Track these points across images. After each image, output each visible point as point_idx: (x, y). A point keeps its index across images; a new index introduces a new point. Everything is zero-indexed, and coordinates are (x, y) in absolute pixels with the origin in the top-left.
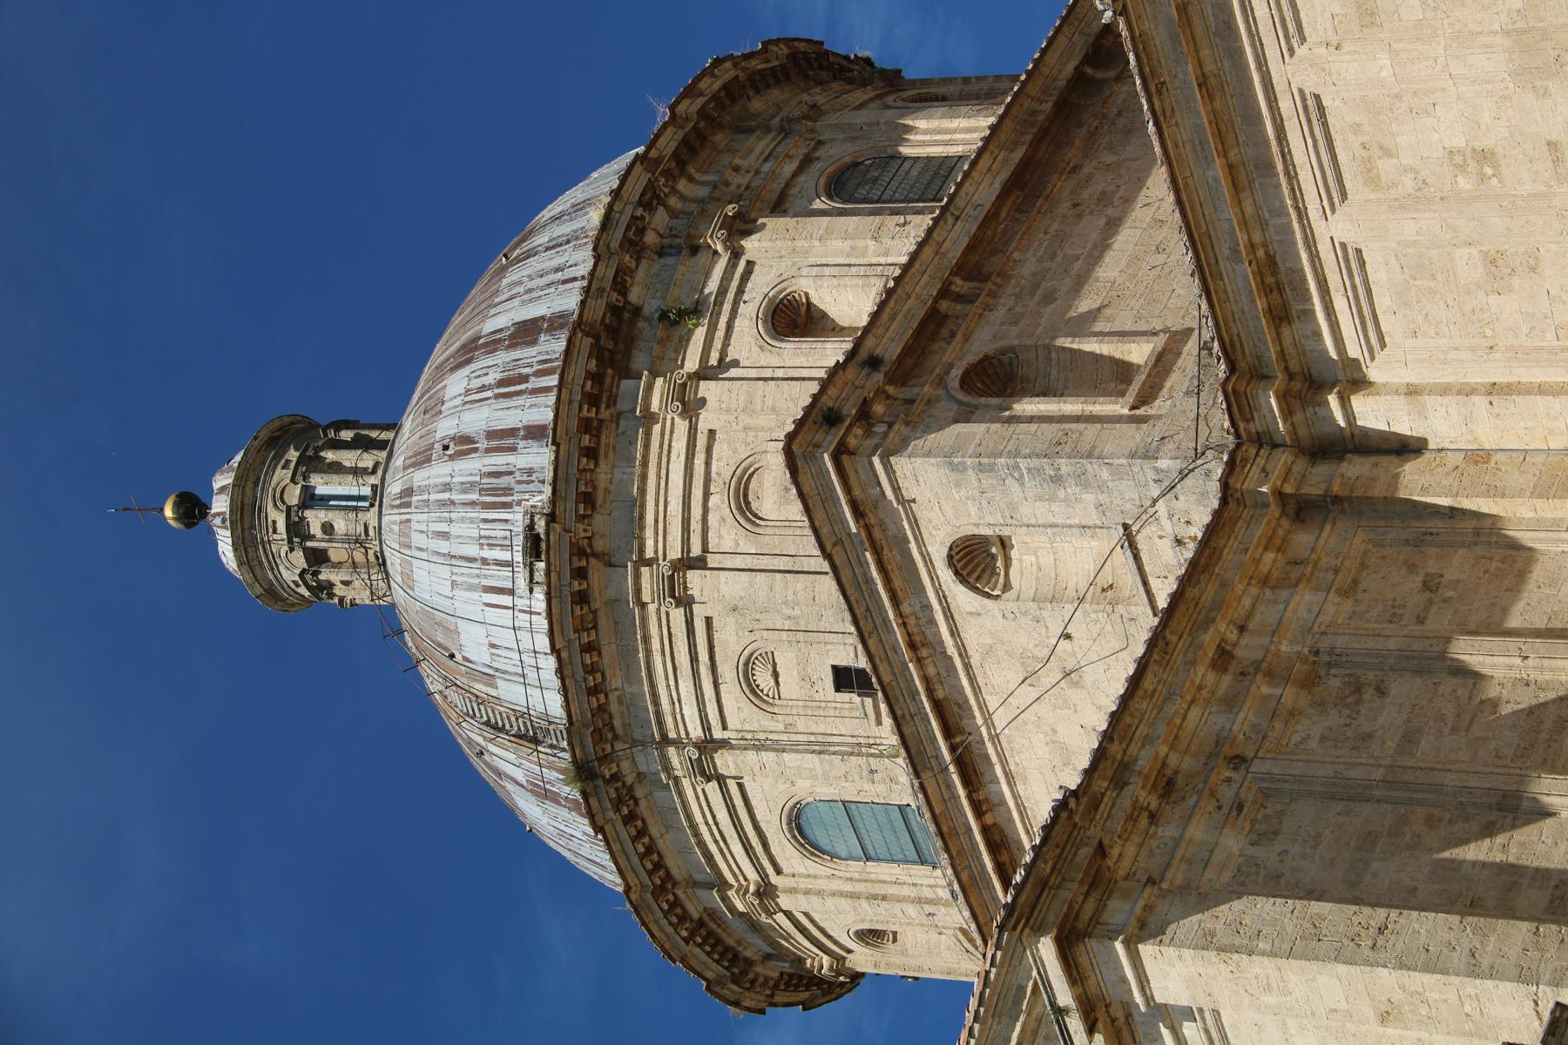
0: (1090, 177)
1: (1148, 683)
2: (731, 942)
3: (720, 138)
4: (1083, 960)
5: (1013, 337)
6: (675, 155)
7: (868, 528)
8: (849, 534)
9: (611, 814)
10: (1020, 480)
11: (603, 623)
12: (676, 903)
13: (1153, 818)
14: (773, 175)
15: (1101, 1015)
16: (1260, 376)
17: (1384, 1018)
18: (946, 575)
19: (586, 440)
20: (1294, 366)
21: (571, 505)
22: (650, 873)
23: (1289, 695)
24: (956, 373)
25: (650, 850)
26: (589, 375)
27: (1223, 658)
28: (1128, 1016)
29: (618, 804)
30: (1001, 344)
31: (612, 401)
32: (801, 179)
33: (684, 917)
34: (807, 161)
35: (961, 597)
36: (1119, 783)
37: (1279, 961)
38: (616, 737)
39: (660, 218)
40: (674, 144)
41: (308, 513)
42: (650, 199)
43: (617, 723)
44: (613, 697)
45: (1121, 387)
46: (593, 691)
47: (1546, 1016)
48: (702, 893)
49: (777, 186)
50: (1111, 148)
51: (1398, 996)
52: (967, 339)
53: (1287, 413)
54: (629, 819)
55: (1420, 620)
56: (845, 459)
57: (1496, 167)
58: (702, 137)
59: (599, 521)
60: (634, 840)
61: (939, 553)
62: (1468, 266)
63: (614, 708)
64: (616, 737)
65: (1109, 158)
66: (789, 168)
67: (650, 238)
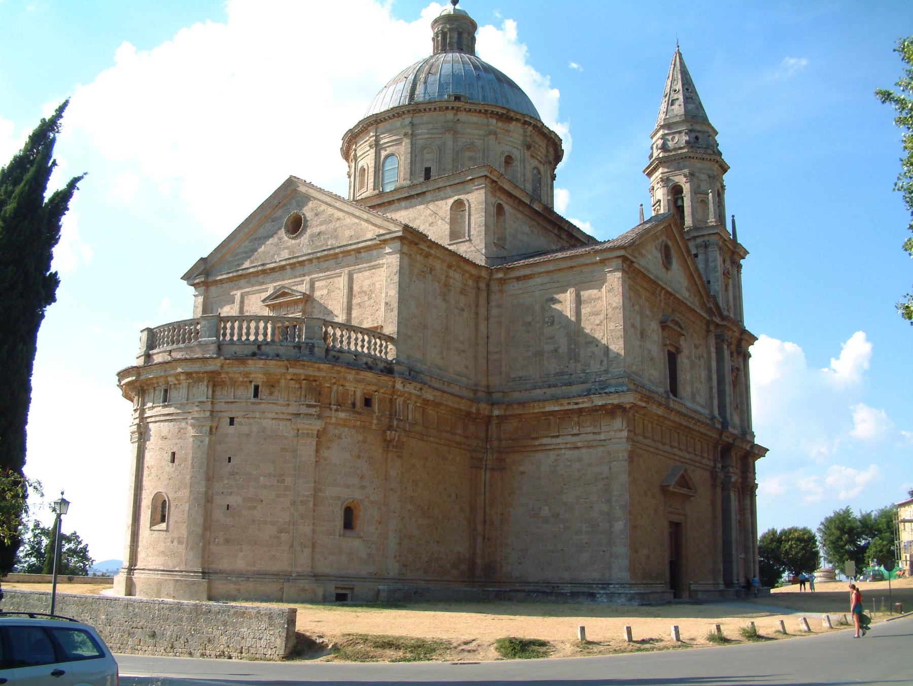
0: (536, 228)
1: (446, 252)
2: (361, 135)
3: (546, 141)
4: (395, 241)
5: (507, 214)
6: (543, 132)
7: (468, 181)
8: (467, 177)
9: (395, 112)
10: (479, 217)
11: (441, 113)
12: (372, 124)
13: (421, 254)
14: (537, 155)
15: (383, 242)
16: (505, 273)
17: (387, 304)
18: (456, 198)
19: (483, 111)
20: (507, 281)
21: (468, 107)
22: (380, 119)
23: (443, 282)
24: (501, 202)
25: (385, 119)
26: (498, 112)
27: (450, 267)
28: (381, 248)
29: (398, 114)
30: (506, 213)
31: (491, 117)
32: (537, 161)
33: (369, 126)
34: (540, 162)
35: (451, 201)
36: (428, 247)
37: (398, 284)
38: (413, 114)
39: (530, 128)
40: (545, 132)
41: (456, 33)
42: (535, 127)
43: (417, 115)
44: (423, 114)
45: (462, 209)
46: (425, 110)
47: (391, 335)
48: (374, 130)
49: (536, 156)
50: (542, 233)
51: (392, 307)
52: (507, 203)
53: (497, 279)
54: (394, 116)
55: (456, 308)
56: (484, 178)
57: (550, 326)
58: (546, 138)
59: (464, 113)
60: (389, 117)
61: (462, 197)
62: (529, 319)
63: (421, 114)
64: (413, 114)
65: (540, 233)
66: (539, 158)
67: (526, 126)
